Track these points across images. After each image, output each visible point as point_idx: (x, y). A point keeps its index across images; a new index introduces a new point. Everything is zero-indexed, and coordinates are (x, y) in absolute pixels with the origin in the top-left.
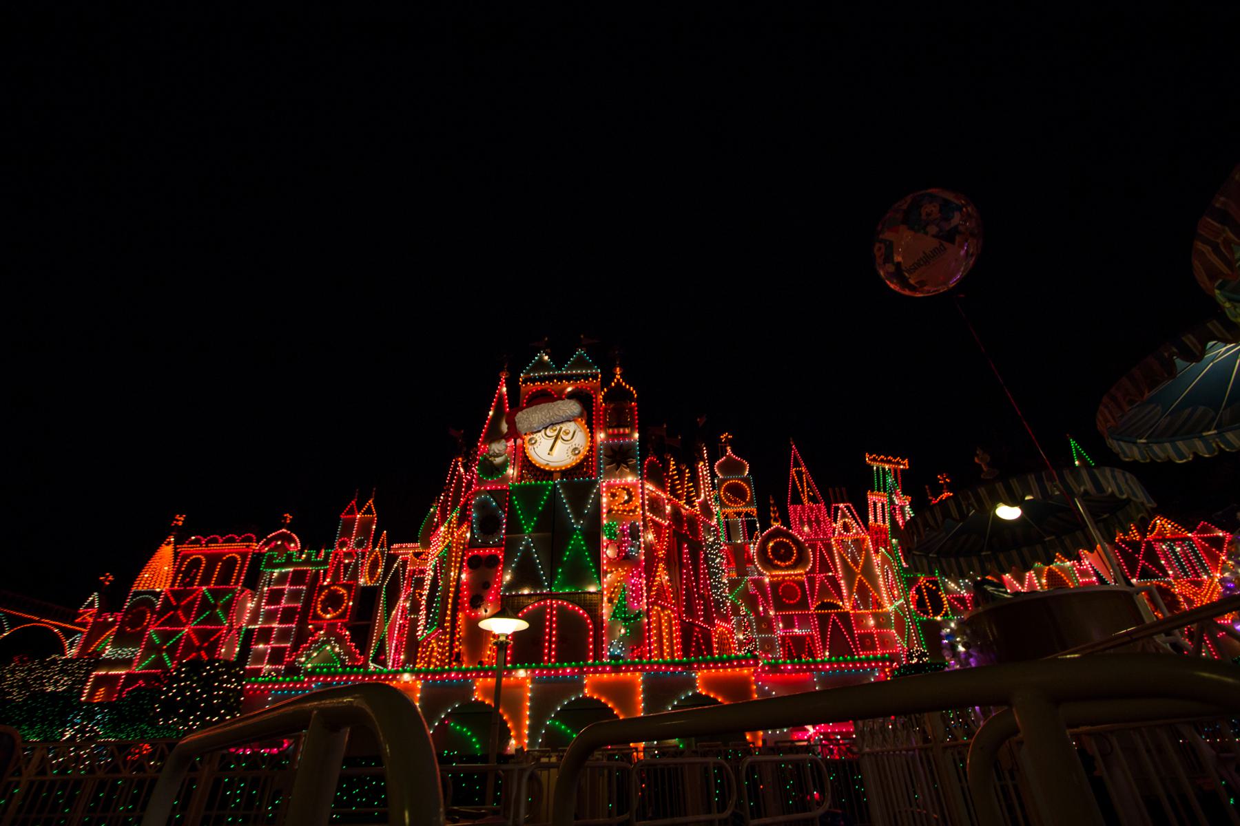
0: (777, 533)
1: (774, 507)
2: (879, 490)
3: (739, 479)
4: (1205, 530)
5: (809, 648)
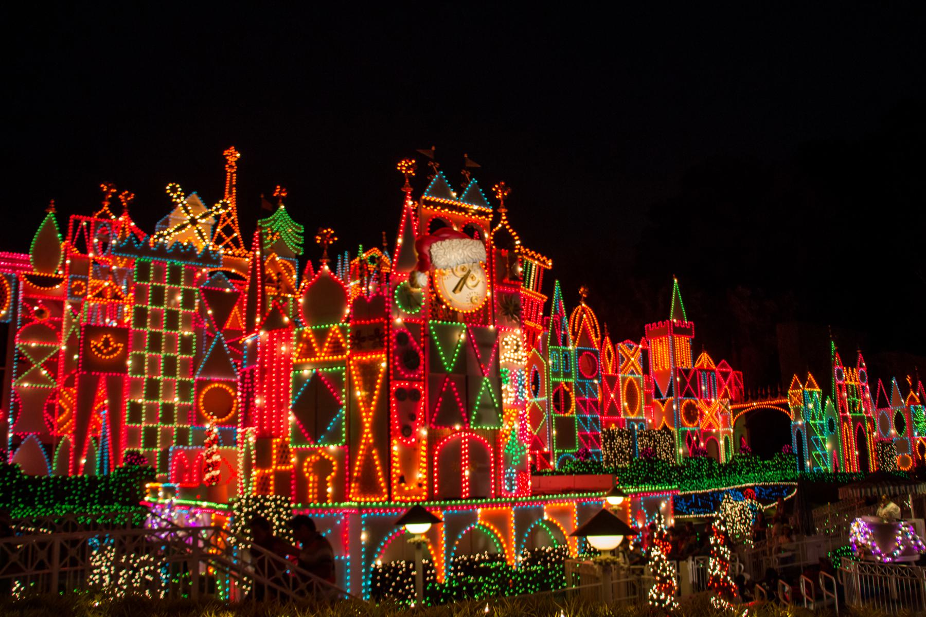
4: (723, 366)
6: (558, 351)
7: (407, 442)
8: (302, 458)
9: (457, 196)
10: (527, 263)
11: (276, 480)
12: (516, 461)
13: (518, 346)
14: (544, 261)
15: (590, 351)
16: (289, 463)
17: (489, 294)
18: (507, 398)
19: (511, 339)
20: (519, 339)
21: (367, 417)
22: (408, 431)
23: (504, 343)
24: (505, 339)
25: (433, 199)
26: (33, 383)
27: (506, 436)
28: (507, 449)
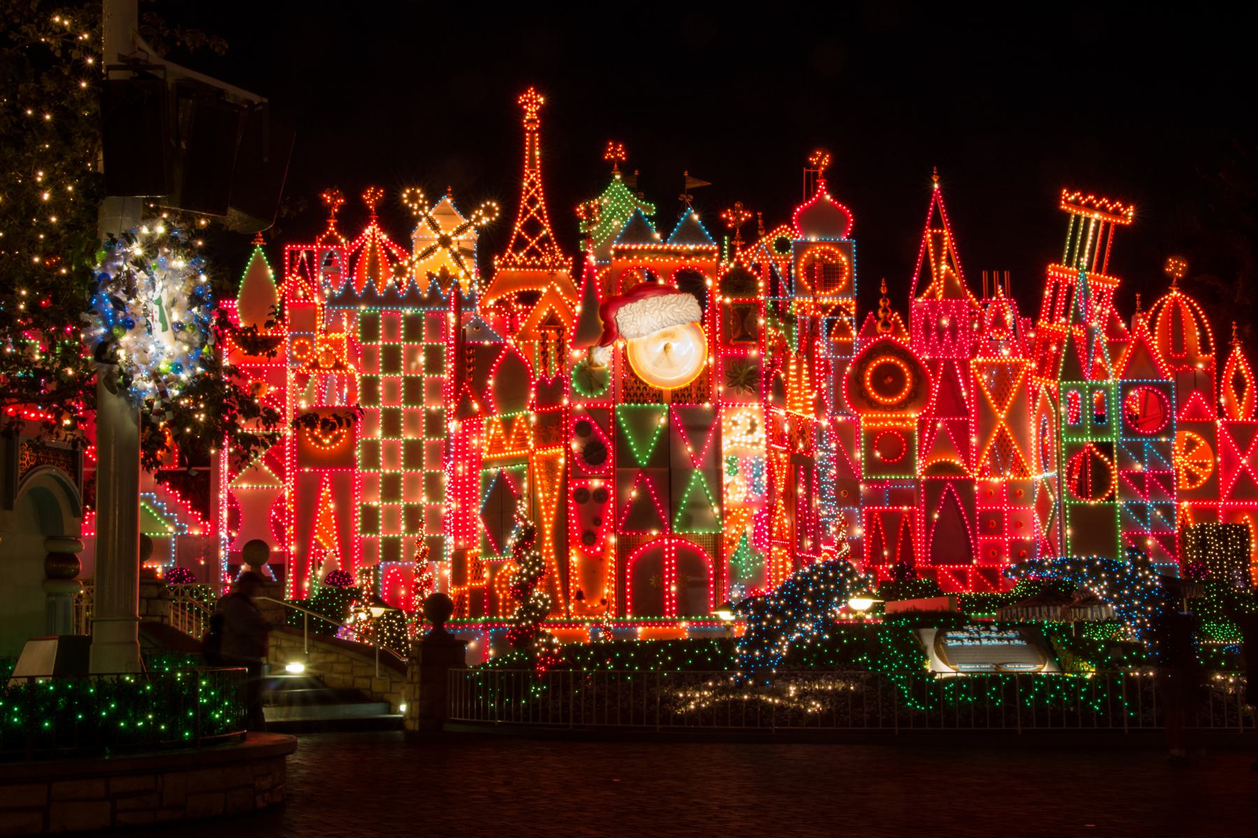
0: (888, 347)
1: (885, 301)
2: (1069, 264)
3: (831, 244)
5: (906, 527)
6: (1081, 389)
7: (589, 551)
8: (493, 574)
9: (662, 238)
10: (1078, 218)
11: (471, 599)
12: (747, 573)
13: (753, 425)
15: (1152, 385)
16: (483, 579)
17: (711, 360)
18: (734, 495)
19: (742, 417)
20: (754, 417)
21: (549, 522)
22: (590, 538)
23: (730, 424)
25: (626, 247)
26: (253, 483)
27: (732, 543)
28: (733, 559)
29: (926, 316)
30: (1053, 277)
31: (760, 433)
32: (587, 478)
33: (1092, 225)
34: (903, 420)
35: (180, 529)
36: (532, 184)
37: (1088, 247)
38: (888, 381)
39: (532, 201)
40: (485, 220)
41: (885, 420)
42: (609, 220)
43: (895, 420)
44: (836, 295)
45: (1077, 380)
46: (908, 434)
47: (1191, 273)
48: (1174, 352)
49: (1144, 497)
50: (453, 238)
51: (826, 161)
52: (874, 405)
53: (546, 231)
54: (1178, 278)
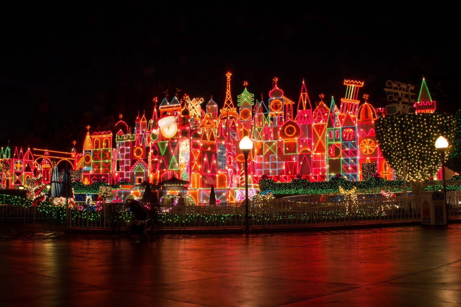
2: (347, 98)
5: (295, 166)
10: (349, 86)
13: (187, 145)
14: (359, 83)
17: (179, 130)
24: (182, 143)
29: (301, 114)
30: (343, 102)
31: (188, 146)
32: (154, 158)
33: (353, 88)
34: (294, 140)
35: (145, 170)
36: (228, 93)
37: (352, 93)
38: (290, 131)
39: (228, 97)
40: (201, 102)
41: (289, 140)
42: (244, 99)
43: (291, 140)
44: (279, 111)
45: (331, 128)
46: (295, 144)
47: (369, 98)
48: (365, 118)
49: (349, 156)
50: (195, 107)
51: (277, 80)
52: (287, 137)
53: (231, 102)
54: (367, 99)
